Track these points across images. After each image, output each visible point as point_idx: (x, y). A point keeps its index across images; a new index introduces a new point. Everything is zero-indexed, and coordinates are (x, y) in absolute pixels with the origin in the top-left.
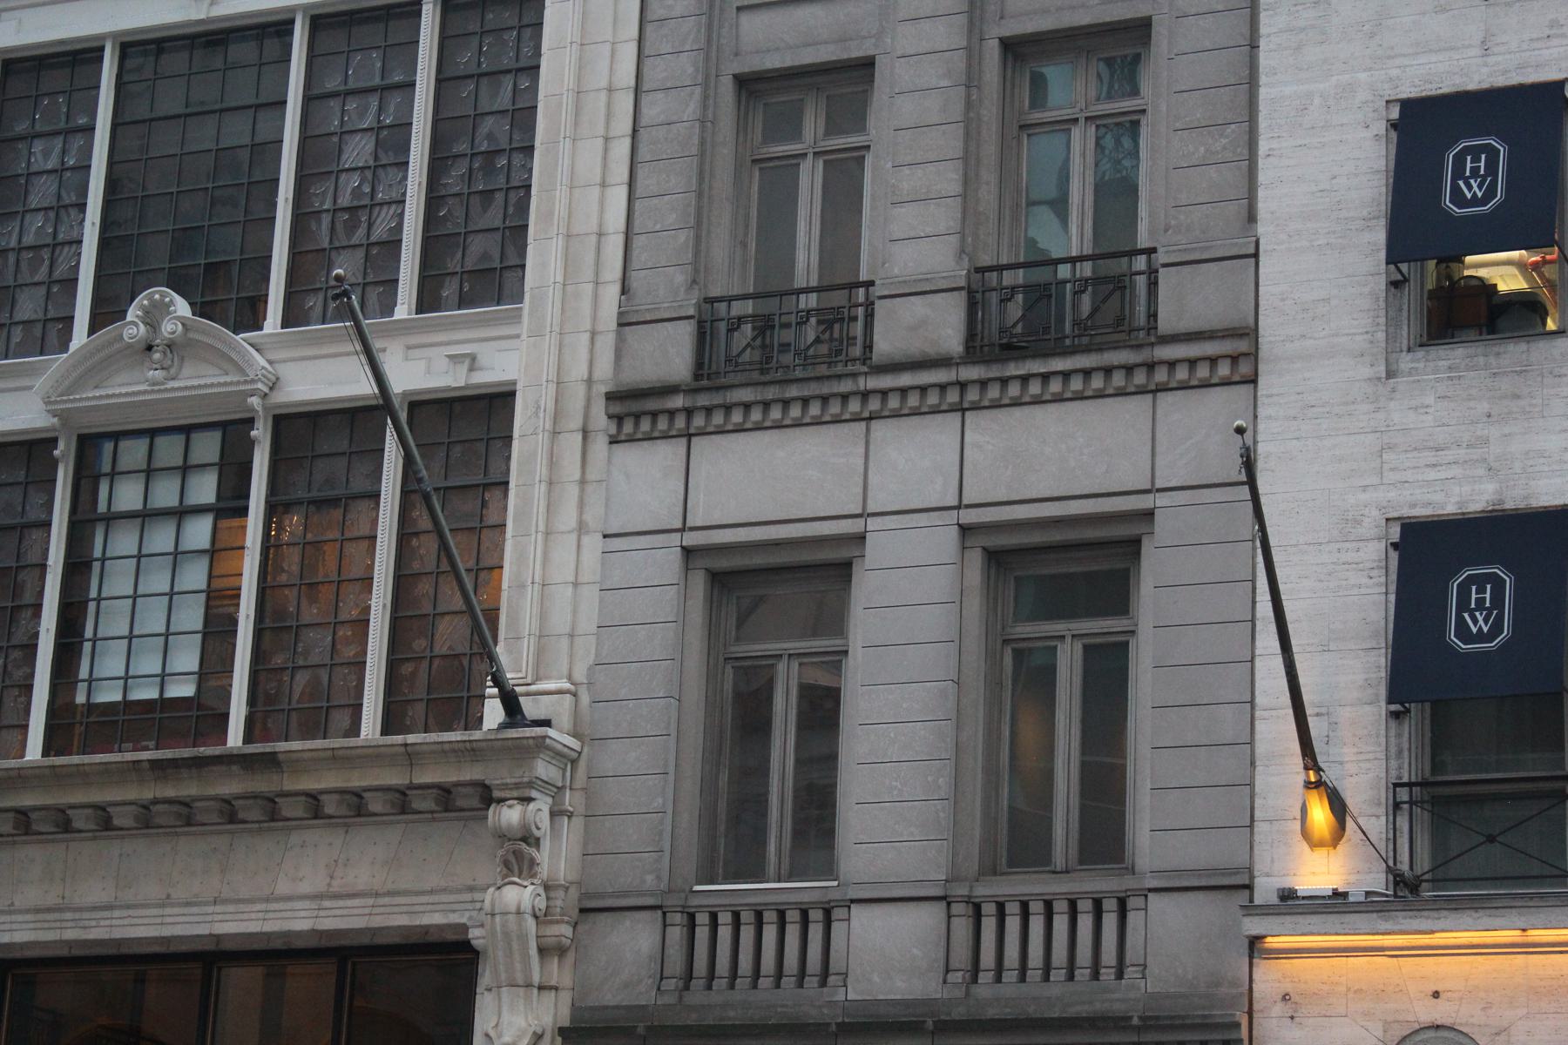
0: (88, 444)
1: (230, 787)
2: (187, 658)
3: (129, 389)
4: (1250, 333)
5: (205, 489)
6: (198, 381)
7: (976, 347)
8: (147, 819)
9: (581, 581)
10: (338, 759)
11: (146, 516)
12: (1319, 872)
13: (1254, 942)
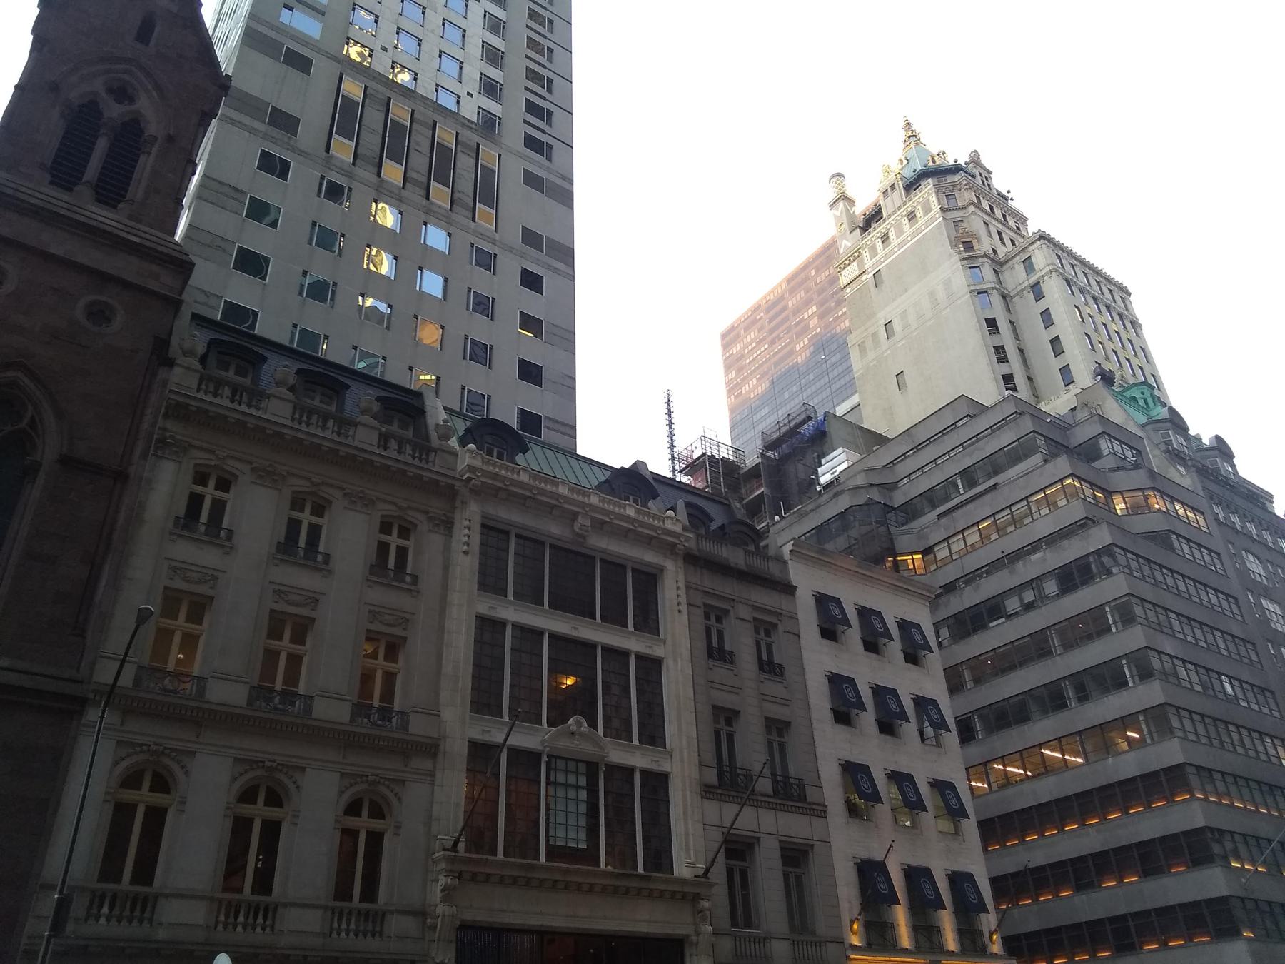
2: (583, 836)
3: (566, 745)
5: (583, 781)
6: (584, 748)
7: (776, 793)
8: (604, 889)
11: (566, 786)
12: (855, 941)
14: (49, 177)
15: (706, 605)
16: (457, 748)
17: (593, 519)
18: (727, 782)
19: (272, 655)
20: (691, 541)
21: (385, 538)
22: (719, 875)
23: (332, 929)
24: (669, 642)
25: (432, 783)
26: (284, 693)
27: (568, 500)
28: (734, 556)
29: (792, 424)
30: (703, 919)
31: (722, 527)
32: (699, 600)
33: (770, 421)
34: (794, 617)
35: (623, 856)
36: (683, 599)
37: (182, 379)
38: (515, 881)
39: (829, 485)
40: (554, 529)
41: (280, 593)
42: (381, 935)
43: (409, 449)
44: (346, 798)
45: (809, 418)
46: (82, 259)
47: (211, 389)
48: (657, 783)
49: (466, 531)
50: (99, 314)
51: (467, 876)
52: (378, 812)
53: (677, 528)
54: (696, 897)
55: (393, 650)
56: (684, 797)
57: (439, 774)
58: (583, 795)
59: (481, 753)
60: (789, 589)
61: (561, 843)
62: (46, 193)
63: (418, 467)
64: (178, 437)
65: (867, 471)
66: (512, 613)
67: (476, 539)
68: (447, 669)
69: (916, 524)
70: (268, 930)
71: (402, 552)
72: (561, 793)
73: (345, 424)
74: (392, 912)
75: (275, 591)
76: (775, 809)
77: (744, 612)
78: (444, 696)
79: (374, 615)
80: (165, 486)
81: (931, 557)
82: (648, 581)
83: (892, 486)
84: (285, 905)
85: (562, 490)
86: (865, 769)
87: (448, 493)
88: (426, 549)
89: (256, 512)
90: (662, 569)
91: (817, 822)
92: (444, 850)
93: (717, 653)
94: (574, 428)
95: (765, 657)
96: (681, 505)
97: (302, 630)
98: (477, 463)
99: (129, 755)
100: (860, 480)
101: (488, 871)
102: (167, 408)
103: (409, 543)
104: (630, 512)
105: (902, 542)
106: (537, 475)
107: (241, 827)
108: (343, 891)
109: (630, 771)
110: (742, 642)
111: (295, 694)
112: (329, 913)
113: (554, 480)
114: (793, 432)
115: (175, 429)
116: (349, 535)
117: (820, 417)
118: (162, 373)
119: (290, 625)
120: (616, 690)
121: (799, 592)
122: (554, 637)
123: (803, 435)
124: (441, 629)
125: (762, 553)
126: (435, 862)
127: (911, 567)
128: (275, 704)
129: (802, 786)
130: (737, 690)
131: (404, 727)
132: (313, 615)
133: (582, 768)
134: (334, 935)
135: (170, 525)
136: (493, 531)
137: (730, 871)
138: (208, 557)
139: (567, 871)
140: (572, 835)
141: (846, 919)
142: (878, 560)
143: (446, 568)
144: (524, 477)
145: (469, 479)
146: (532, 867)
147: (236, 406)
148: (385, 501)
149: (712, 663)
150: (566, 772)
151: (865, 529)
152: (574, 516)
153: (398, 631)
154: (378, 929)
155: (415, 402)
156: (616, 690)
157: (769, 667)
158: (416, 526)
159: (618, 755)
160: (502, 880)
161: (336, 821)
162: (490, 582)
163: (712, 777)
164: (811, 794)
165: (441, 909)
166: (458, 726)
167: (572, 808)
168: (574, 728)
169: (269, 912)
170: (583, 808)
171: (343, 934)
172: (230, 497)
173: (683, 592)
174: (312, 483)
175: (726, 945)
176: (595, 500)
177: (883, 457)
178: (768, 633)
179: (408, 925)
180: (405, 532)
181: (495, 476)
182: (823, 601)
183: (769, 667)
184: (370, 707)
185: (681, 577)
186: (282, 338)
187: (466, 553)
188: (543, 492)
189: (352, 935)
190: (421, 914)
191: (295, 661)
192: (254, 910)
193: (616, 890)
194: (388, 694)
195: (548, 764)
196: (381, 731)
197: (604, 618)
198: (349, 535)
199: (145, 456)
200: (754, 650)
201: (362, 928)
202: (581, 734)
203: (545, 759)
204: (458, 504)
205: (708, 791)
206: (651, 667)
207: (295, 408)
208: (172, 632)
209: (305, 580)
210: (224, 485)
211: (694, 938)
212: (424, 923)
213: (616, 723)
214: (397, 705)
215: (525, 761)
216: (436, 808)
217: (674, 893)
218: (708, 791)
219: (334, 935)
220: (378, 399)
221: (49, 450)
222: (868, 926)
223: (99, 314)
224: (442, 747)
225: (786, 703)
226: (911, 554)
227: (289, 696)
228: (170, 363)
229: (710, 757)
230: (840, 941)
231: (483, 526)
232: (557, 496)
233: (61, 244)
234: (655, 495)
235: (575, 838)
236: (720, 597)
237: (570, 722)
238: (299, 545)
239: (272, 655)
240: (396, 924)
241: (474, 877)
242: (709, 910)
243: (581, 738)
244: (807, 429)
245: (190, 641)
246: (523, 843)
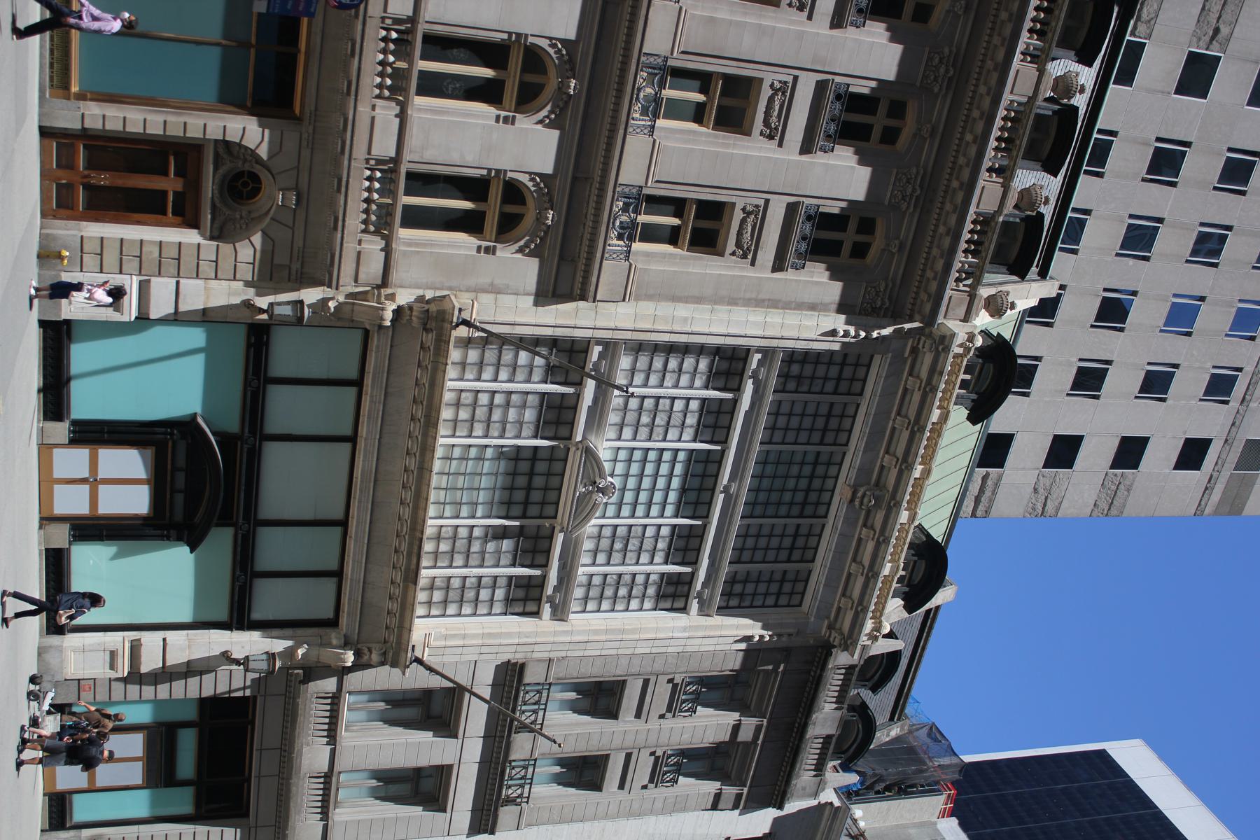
4: (492, 833)
26: (657, 100)
42: (364, 231)
70: (377, 91)
75: (785, 83)
78: (647, 307)
85: (918, 471)
92: (460, 310)
111: (656, 115)
124: (733, 302)
144: (935, 415)
155: (1034, 269)
161: (498, 171)
176: (904, 516)
184: (637, 211)
192: (400, 77)
214: (637, 246)
234: (910, 606)
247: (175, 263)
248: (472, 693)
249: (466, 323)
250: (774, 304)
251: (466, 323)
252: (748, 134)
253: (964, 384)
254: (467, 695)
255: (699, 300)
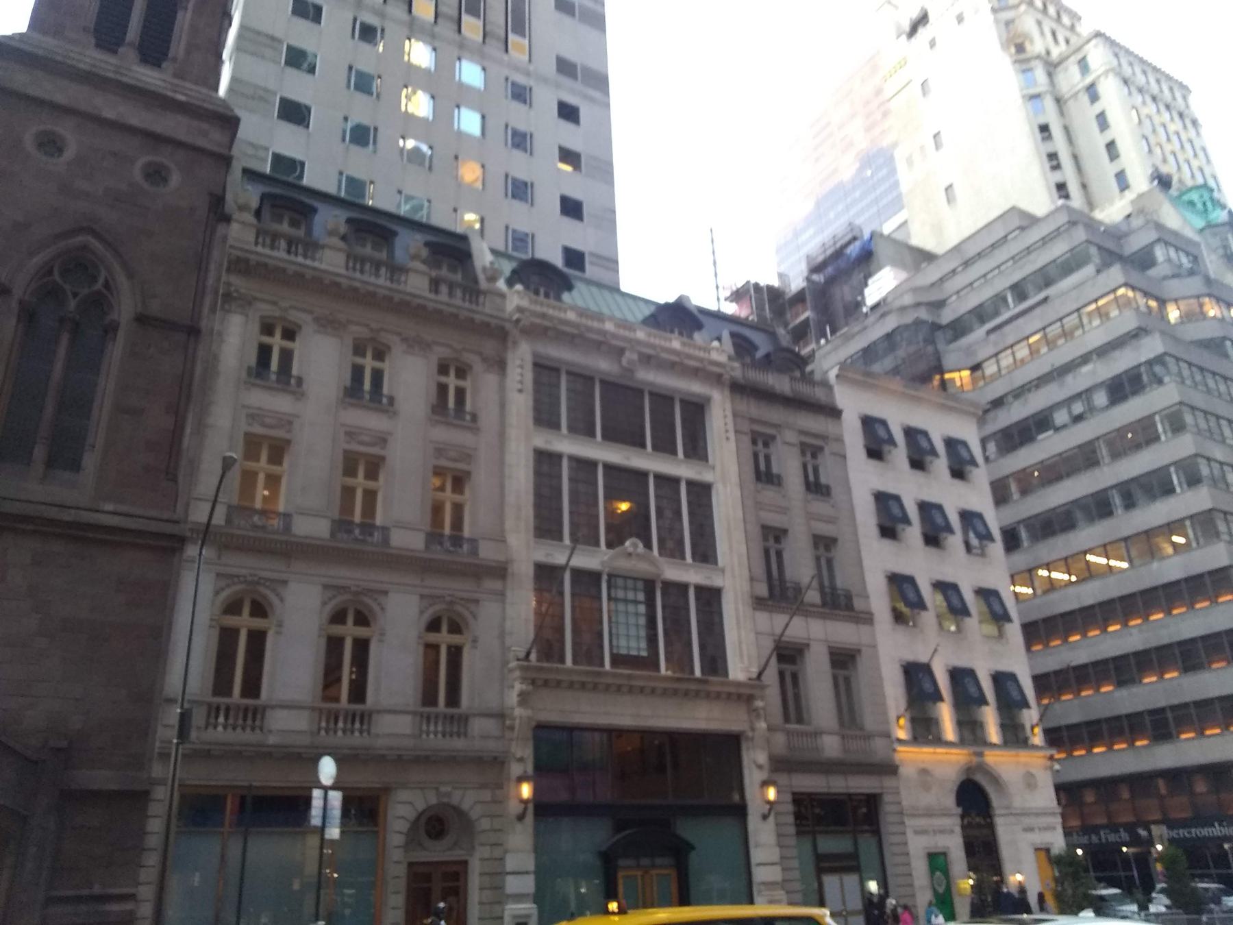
0: (610, 576)
1: (693, 687)
2: (643, 645)
3: (624, 564)
5: (641, 596)
6: (642, 567)
7: (824, 604)
9: (745, 645)
10: (722, 684)
11: (626, 601)
12: (902, 734)
13: (894, 750)
14: (93, 41)
15: (753, 432)
16: (524, 569)
17: (640, 354)
18: (777, 593)
19: (348, 492)
20: (736, 370)
21: (359, 360)
22: (771, 677)
23: (421, 731)
24: (718, 468)
25: (503, 602)
27: (614, 336)
28: (781, 383)
29: (838, 245)
30: (758, 716)
31: (767, 356)
32: (746, 427)
33: (815, 243)
34: (839, 440)
35: (681, 661)
36: (731, 427)
37: (240, 233)
38: (583, 686)
39: (875, 307)
40: (603, 365)
41: (351, 434)
43: (459, 293)
44: (427, 617)
45: (855, 239)
46: (134, 121)
47: (268, 241)
48: (710, 598)
49: (519, 370)
50: (156, 174)
51: (539, 682)
52: (455, 628)
53: (723, 358)
54: (750, 699)
55: (459, 482)
56: (737, 610)
57: (509, 593)
58: (642, 609)
59: (546, 575)
60: (834, 413)
61: (623, 652)
62: (91, 57)
63: (470, 310)
64: (243, 291)
65: (915, 290)
66: (567, 446)
67: (529, 376)
68: (510, 499)
69: (964, 341)
70: (365, 734)
71: (460, 393)
72: (621, 607)
73: (397, 270)
74: (475, 715)
76: (823, 617)
77: (791, 436)
78: (509, 524)
79: (439, 451)
80: (234, 338)
81: (979, 373)
82: (696, 411)
83: (940, 305)
84: (379, 712)
85: (609, 326)
86: (911, 580)
87: (499, 334)
88: (483, 390)
89: (321, 359)
90: (708, 400)
91: (864, 629)
92: (518, 660)
93: (765, 476)
94: (617, 262)
95: (811, 478)
96: (726, 335)
97: (374, 467)
98: (525, 303)
99: (228, 586)
100: (908, 300)
101: (559, 677)
102: (229, 262)
103: (467, 384)
104: (676, 344)
105: (949, 360)
106: (583, 313)
107: (334, 645)
108: (429, 698)
109: (683, 587)
110: (789, 464)
111: (373, 526)
112: (418, 718)
113: (600, 317)
114: (839, 254)
115: (239, 283)
116: (410, 377)
117: (866, 236)
118: (221, 229)
119: (363, 463)
120: (668, 513)
121: (844, 415)
122: (609, 468)
123: (849, 257)
124: (502, 462)
125: (808, 379)
126: (511, 671)
127: (958, 384)
128: (356, 535)
129: (849, 597)
130: (784, 510)
131: (474, 552)
132: (382, 453)
133: (640, 585)
134: (424, 736)
135: (244, 374)
136: (545, 370)
137: (781, 674)
138: (281, 403)
139: (630, 677)
140: (633, 644)
141: (892, 714)
142: (925, 379)
143: (503, 405)
144: (571, 316)
145: (518, 321)
146: (599, 674)
147: (292, 258)
148: (358, 324)
149: (760, 486)
150: (625, 588)
151: (912, 349)
152: (621, 352)
153: (461, 466)
154: (462, 730)
156: (668, 513)
157: (816, 488)
158: (471, 367)
159: (672, 572)
160: (571, 685)
162: (545, 417)
163: (763, 590)
164: (858, 604)
165: (518, 712)
166: (523, 549)
167: (632, 620)
168: (631, 550)
169: (365, 718)
170: (642, 621)
171: (432, 736)
172: (296, 346)
173: (730, 420)
174: (372, 330)
175: (780, 739)
176: (641, 335)
177: (931, 274)
178: (814, 456)
179: (490, 726)
180: (461, 373)
181: (544, 316)
182: (869, 423)
183: (816, 488)
184: (442, 535)
185: (728, 406)
186: (331, 189)
187: (520, 391)
188: (589, 329)
189: (440, 736)
190: (501, 716)
191: (370, 496)
193: (675, 692)
194: (458, 523)
195: (609, 582)
196: (454, 558)
197: (655, 448)
198: (410, 377)
199: (213, 310)
200: (752, 461)
201: (448, 730)
202: (638, 555)
203: (605, 578)
204: (510, 344)
205: (759, 603)
206: (701, 492)
207: (348, 257)
208: (256, 474)
209: (373, 421)
210: (289, 334)
211: (750, 734)
212: (504, 723)
213: (670, 544)
214: (467, 533)
215: (587, 580)
216: (508, 624)
217: (729, 695)
218: (759, 603)
219: (424, 736)
220: (427, 244)
221: (125, 308)
222: (914, 721)
223: (156, 174)
224: (510, 570)
225: (831, 520)
226: (959, 370)
227: (368, 527)
228: (227, 219)
229: (760, 571)
230: (887, 735)
231: (536, 365)
232: (604, 333)
233: (112, 108)
234: (699, 326)
235: (638, 647)
236: (765, 423)
237: (627, 543)
238: (364, 389)
239: (348, 492)
240: (478, 726)
241: (546, 683)
242: (764, 709)
243: (635, 557)
244: (853, 250)
245: (273, 481)
246: (589, 652)
247: (496, 876)
248: (782, 635)
249: (528, 654)
250: (502, 435)
251: (528, 654)
252: (383, 458)
253: (547, 296)
254: (784, 639)
255: (502, 487)
